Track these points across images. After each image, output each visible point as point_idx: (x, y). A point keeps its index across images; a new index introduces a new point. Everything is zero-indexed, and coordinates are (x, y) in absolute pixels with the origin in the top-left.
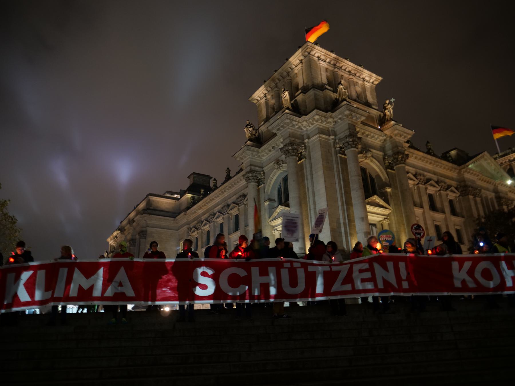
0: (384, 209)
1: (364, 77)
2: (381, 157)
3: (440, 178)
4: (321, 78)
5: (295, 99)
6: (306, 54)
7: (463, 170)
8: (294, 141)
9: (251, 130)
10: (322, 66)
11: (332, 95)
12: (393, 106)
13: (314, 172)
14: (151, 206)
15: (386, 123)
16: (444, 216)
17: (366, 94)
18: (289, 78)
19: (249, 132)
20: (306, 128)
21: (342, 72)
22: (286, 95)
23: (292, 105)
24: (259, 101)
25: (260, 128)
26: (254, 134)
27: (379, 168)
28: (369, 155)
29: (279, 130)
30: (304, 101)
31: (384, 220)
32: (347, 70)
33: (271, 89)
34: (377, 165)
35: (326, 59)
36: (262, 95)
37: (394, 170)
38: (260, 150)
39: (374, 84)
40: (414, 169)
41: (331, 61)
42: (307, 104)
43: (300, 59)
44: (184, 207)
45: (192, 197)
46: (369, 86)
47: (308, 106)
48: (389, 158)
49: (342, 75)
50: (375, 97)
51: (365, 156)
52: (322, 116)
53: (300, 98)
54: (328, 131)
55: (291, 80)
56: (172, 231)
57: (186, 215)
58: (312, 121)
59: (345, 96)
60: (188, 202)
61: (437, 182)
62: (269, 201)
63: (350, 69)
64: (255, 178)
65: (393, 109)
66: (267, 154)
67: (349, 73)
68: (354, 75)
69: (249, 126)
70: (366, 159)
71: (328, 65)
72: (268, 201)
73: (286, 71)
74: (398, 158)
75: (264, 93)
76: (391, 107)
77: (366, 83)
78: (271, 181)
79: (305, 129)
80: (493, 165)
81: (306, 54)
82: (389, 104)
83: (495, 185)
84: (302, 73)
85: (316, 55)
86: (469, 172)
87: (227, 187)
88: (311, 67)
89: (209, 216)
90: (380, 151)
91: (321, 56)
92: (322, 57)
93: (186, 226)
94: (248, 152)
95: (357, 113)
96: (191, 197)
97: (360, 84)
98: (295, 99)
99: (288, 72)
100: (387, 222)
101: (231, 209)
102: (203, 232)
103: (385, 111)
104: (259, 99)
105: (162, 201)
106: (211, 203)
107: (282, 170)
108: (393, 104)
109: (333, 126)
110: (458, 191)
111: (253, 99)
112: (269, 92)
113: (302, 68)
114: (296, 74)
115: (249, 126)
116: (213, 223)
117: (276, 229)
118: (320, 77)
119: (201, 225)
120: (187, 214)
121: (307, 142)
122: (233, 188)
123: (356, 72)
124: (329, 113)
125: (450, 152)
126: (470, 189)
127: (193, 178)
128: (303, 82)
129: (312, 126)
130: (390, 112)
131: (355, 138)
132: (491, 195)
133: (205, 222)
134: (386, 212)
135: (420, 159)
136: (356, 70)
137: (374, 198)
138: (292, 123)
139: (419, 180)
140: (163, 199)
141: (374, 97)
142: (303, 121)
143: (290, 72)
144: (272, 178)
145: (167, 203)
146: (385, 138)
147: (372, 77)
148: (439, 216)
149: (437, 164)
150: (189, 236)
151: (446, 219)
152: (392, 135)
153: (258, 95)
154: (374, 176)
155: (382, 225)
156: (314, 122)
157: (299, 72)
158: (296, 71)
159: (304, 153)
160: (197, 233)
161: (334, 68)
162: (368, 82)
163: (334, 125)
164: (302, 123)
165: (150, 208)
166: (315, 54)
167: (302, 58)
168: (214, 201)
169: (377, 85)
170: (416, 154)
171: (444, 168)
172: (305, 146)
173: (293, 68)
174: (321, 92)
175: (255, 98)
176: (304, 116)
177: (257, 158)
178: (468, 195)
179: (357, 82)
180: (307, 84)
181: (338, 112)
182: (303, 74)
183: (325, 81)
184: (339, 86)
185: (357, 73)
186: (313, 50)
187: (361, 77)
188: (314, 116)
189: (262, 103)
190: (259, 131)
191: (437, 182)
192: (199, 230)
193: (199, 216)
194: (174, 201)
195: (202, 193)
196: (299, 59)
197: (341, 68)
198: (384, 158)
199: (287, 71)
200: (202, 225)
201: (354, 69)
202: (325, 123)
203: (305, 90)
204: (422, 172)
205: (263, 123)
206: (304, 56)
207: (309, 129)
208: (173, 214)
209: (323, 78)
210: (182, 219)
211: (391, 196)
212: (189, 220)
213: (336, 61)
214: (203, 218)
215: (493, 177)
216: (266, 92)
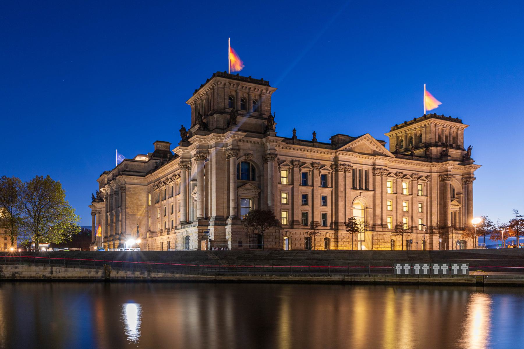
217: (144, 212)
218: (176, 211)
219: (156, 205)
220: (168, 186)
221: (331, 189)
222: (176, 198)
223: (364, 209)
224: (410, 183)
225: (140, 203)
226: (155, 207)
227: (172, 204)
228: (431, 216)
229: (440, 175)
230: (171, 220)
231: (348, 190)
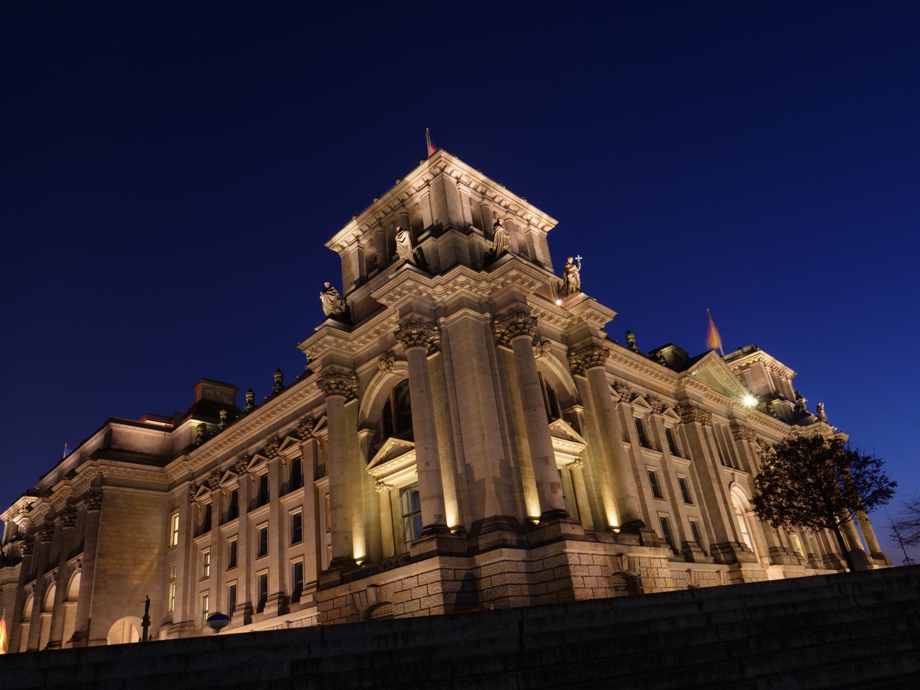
0: (575, 443)
1: (529, 219)
2: (564, 353)
3: (651, 391)
4: (463, 214)
5: (418, 247)
6: (438, 170)
7: (683, 380)
8: (420, 319)
9: (332, 298)
10: (464, 194)
11: (483, 243)
12: (580, 269)
13: (456, 377)
14: (114, 444)
15: (569, 296)
16: (661, 456)
17: (533, 246)
18: (402, 210)
19: (329, 302)
20: (440, 297)
21: (494, 206)
22: (404, 239)
23: (415, 255)
24: (346, 249)
25: (349, 297)
26: (338, 307)
27: (562, 371)
28: (547, 349)
29: (392, 299)
30: (435, 251)
31: (575, 462)
32: (503, 204)
33: (368, 228)
34: (558, 367)
35: (470, 183)
36: (352, 238)
37: (583, 375)
38: (351, 336)
39: (545, 232)
40: (612, 376)
41: (477, 187)
42: (440, 256)
43: (426, 179)
44: (182, 445)
45: (199, 426)
46: (537, 234)
47: (441, 260)
48: (577, 354)
49: (495, 213)
50: (547, 252)
51: (540, 350)
52: (470, 277)
53: (428, 244)
54: (478, 303)
55: (408, 213)
56: (156, 492)
57: (187, 460)
58: (454, 285)
59: (507, 247)
60: (191, 436)
61: (647, 399)
62: (368, 430)
63: (508, 203)
64: (341, 387)
65: (579, 272)
66: (364, 342)
67: (506, 210)
68: (515, 213)
69: (329, 291)
70: (541, 356)
71: (473, 193)
72: (366, 431)
73: (399, 199)
74: (593, 355)
75: (356, 235)
76: (578, 270)
77: (532, 228)
78: (371, 392)
79: (439, 300)
80: (724, 372)
81: (438, 170)
82: (573, 264)
83: (728, 407)
84: (429, 203)
85: (454, 174)
86: (692, 384)
87: (279, 406)
88: (445, 194)
89: (238, 462)
90: (563, 343)
91: (461, 176)
92: (464, 179)
93: (187, 483)
94: (329, 338)
95: (530, 276)
96: (198, 426)
97: (522, 230)
98: (418, 247)
99: (403, 200)
100: (580, 467)
101: (286, 447)
102: (225, 493)
103: (568, 276)
104: (345, 245)
105: (137, 434)
106: (242, 438)
107: (394, 373)
108: (580, 264)
109: (488, 296)
110: (679, 415)
111: (334, 244)
112: (366, 233)
113: (429, 194)
114: (417, 204)
115: (330, 292)
116: (245, 475)
117: (383, 482)
118: (460, 210)
119: (220, 480)
120: (191, 459)
121: (443, 322)
122: (290, 408)
123: (517, 209)
124: (483, 273)
125: (662, 350)
126: (696, 411)
127: (203, 390)
128: (431, 219)
129: (452, 295)
130: (576, 278)
131: (527, 318)
132: (725, 422)
133: (228, 473)
134: (578, 448)
135: (620, 359)
136: (518, 204)
137: (559, 424)
138: (417, 288)
139: (621, 394)
140: (141, 431)
141: (546, 252)
142: (436, 286)
143: (407, 201)
144: (373, 388)
145: (146, 437)
146: (569, 320)
147: (542, 219)
148: (653, 457)
149: (646, 368)
150: (192, 502)
151: (663, 462)
152: (581, 315)
153: (342, 238)
154: (553, 387)
155: (571, 471)
156: (457, 287)
157: (423, 200)
158: (417, 200)
159: (437, 341)
160: (211, 496)
161: (483, 199)
162: (536, 227)
163: (489, 294)
164: (434, 289)
165: (113, 446)
166: (452, 172)
167: (430, 177)
168: (249, 433)
169: (549, 232)
170: (616, 351)
171: (657, 376)
172: (440, 330)
173: (412, 194)
174: (465, 236)
175: (337, 243)
176: (439, 276)
177: (345, 351)
178: (693, 421)
179: (518, 226)
180: (439, 222)
181: (497, 271)
182: (430, 205)
183: (469, 219)
184: (497, 228)
185: (518, 210)
186: (449, 166)
187: (525, 217)
188: (458, 276)
189: (351, 252)
190: (347, 302)
191: (647, 399)
192: (216, 489)
193: (215, 463)
194: (163, 433)
195: (223, 418)
196: (423, 179)
197: (494, 199)
198: (569, 356)
199: (401, 199)
200: (222, 481)
201: (515, 202)
202: (475, 290)
203: (436, 231)
204: (624, 381)
205: (353, 287)
206: (434, 175)
207: (445, 300)
208: (162, 458)
209: (465, 213)
210: (178, 469)
212: (194, 471)
213: (487, 188)
214: (224, 466)
215: (726, 393)
216: (360, 233)
217: (154, 568)
218: (281, 543)
219: (199, 541)
220: (248, 478)
221: (688, 463)
222: (280, 504)
223: (742, 515)
225: (142, 540)
226: (195, 547)
227: (234, 539)
230: (256, 576)
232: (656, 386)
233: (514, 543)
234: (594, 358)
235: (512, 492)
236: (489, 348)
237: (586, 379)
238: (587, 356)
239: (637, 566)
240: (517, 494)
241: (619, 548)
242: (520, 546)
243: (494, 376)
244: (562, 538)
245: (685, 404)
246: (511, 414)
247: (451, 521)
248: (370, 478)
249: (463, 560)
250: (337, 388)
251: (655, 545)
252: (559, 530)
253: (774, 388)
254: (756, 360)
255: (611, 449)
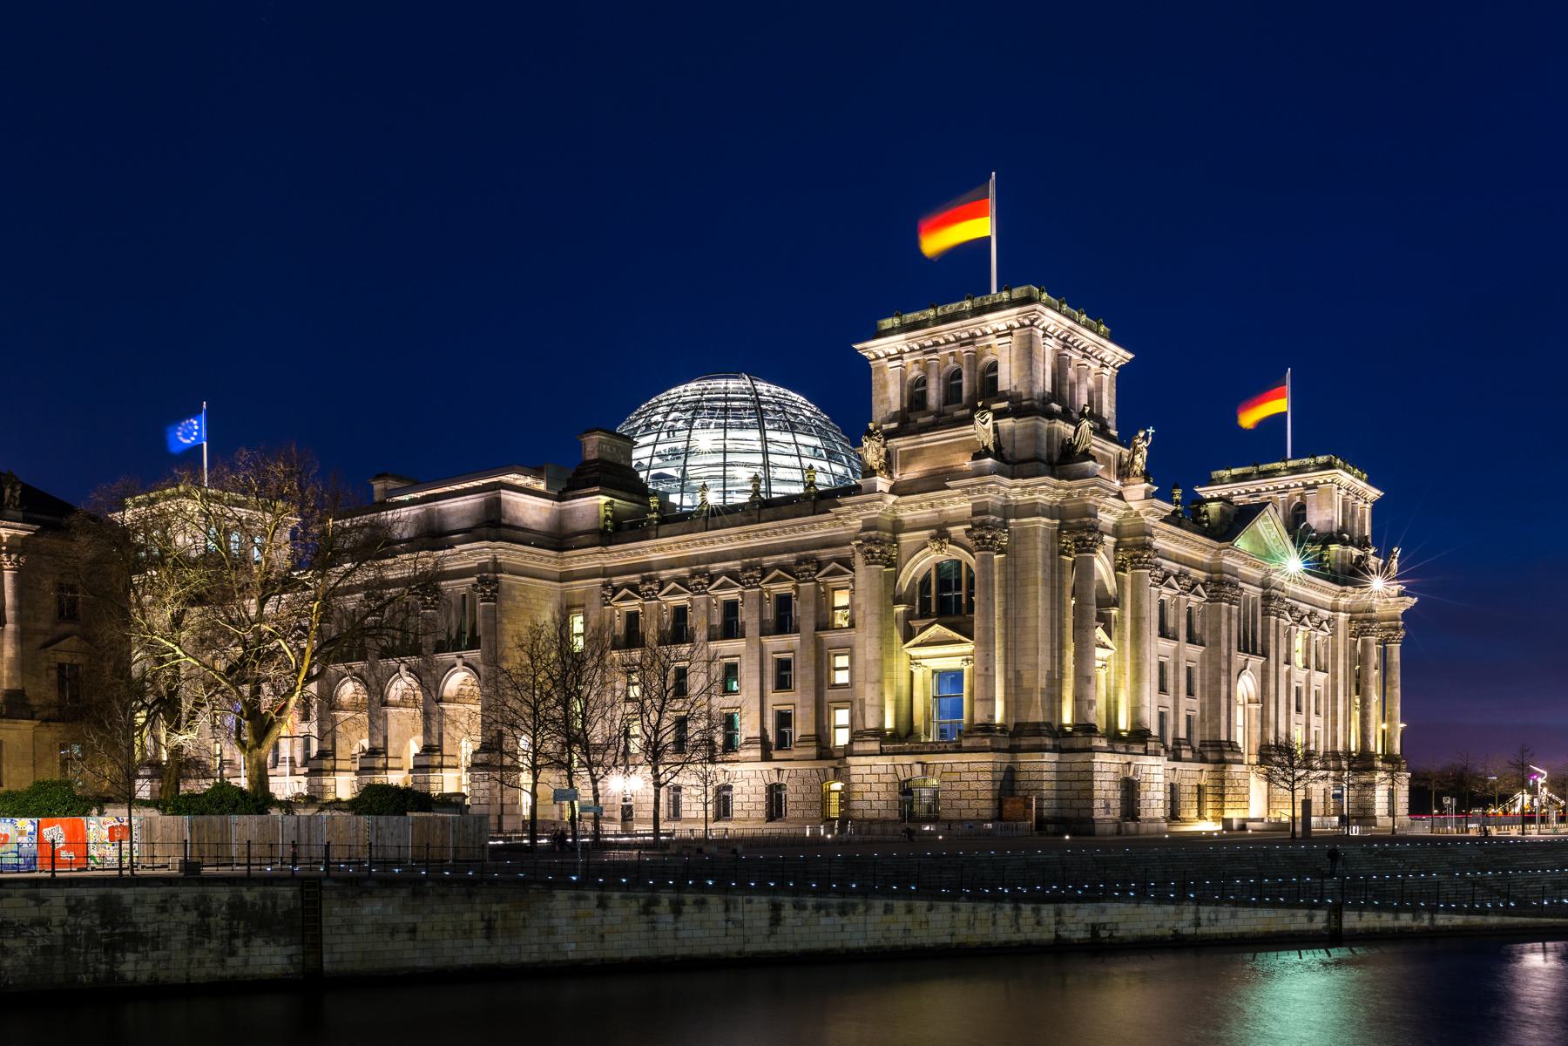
3: (1183, 567)
48: (1124, 551)
56: (549, 582)
78: (914, 565)
96: (606, 504)
144: (917, 562)
145: (534, 508)
150: (605, 605)
151: (1177, 652)
195: (655, 508)
211: (1115, 622)
224: (1307, 635)
228: (1335, 724)
229: (1351, 620)
231: (1234, 651)
232: (1190, 558)
233: (1051, 747)
234: (1143, 560)
235: (1052, 701)
236: (1052, 557)
237: (1126, 575)
238: (1135, 556)
239: (1140, 773)
240: (1057, 704)
241: (1129, 758)
242: (1054, 750)
243: (1053, 588)
244: (1091, 750)
245: (1217, 579)
246: (1062, 627)
247: (999, 718)
248: (904, 654)
249: (1008, 755)
250: (880, 557)
251: (1157, 754)
252: (1091, 743)
253: (1340, 524)
254: (1329, 480)
255: (1138, 658)
